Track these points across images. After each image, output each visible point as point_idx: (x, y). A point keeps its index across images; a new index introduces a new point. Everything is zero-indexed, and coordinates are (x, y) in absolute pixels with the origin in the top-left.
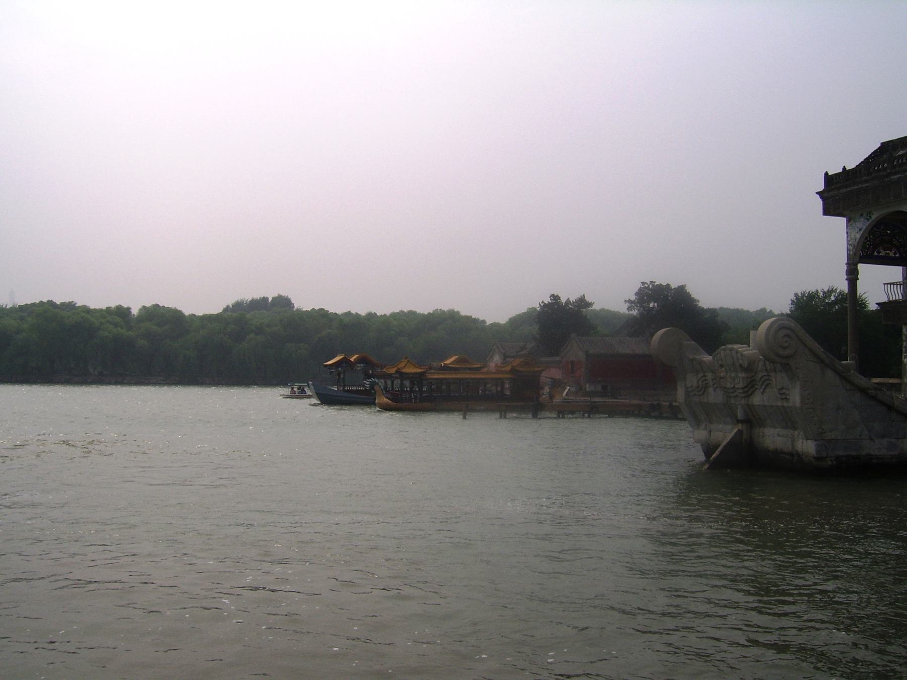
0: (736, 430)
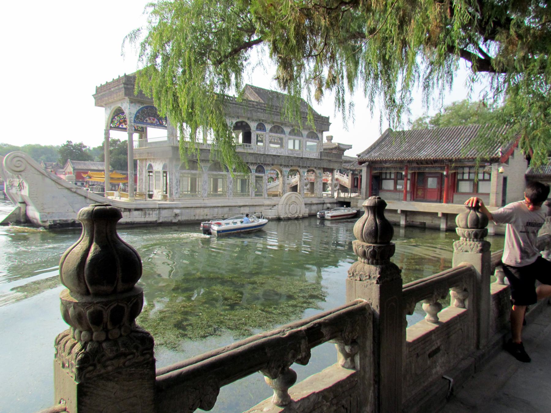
0: (16, 207)
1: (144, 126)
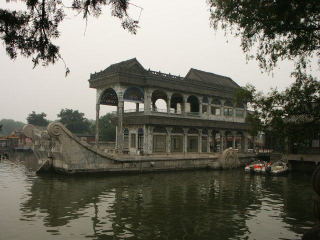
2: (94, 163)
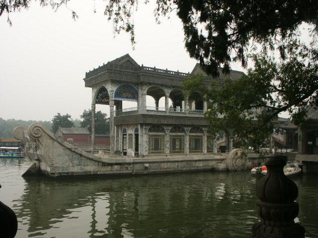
0: (32, 164)
1: (120, 99)
2: (78, 165)
